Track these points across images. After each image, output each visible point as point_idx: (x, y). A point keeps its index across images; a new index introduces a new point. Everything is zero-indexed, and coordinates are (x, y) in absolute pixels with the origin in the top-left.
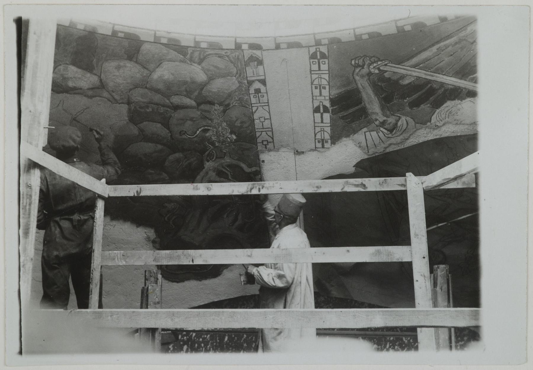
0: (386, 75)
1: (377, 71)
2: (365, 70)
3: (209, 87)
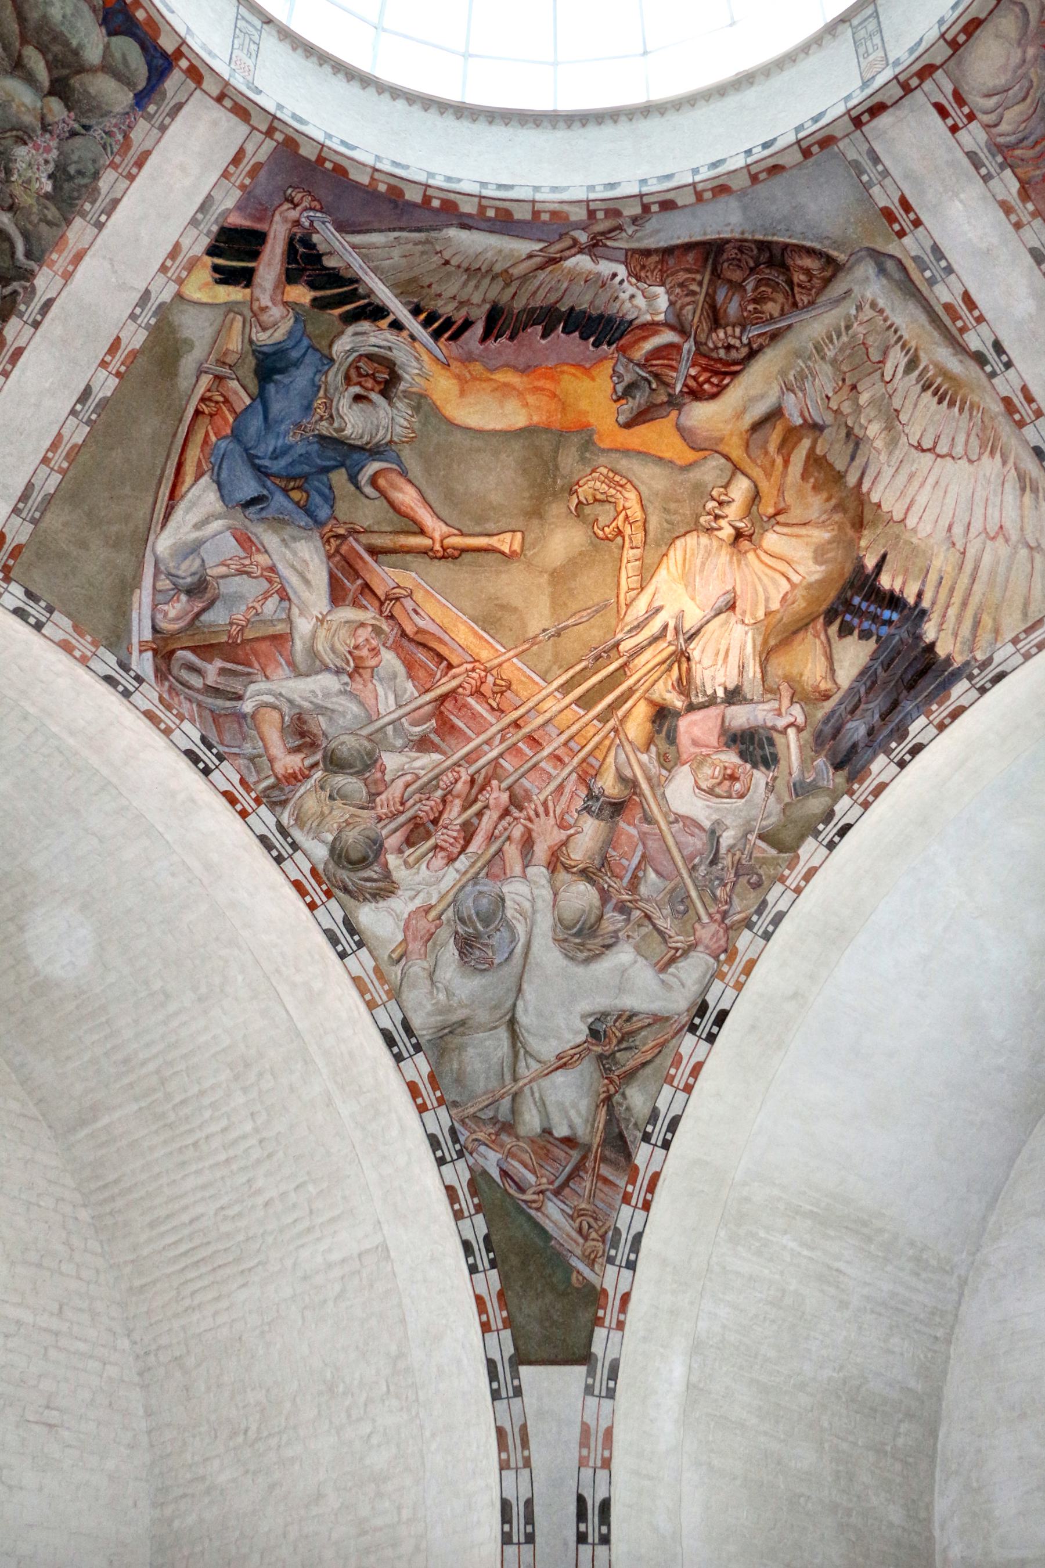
0: (315, 238)
1: (307, 224)
2: (294, 214)
3: (86, 78)
